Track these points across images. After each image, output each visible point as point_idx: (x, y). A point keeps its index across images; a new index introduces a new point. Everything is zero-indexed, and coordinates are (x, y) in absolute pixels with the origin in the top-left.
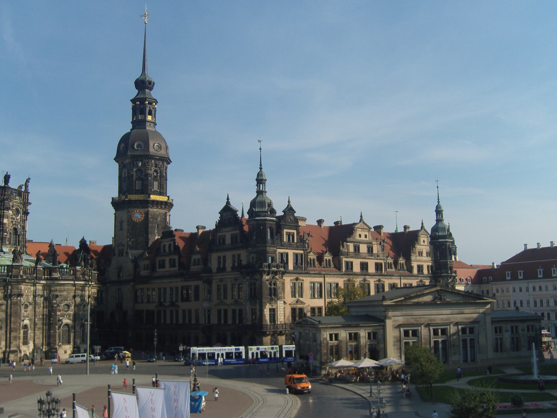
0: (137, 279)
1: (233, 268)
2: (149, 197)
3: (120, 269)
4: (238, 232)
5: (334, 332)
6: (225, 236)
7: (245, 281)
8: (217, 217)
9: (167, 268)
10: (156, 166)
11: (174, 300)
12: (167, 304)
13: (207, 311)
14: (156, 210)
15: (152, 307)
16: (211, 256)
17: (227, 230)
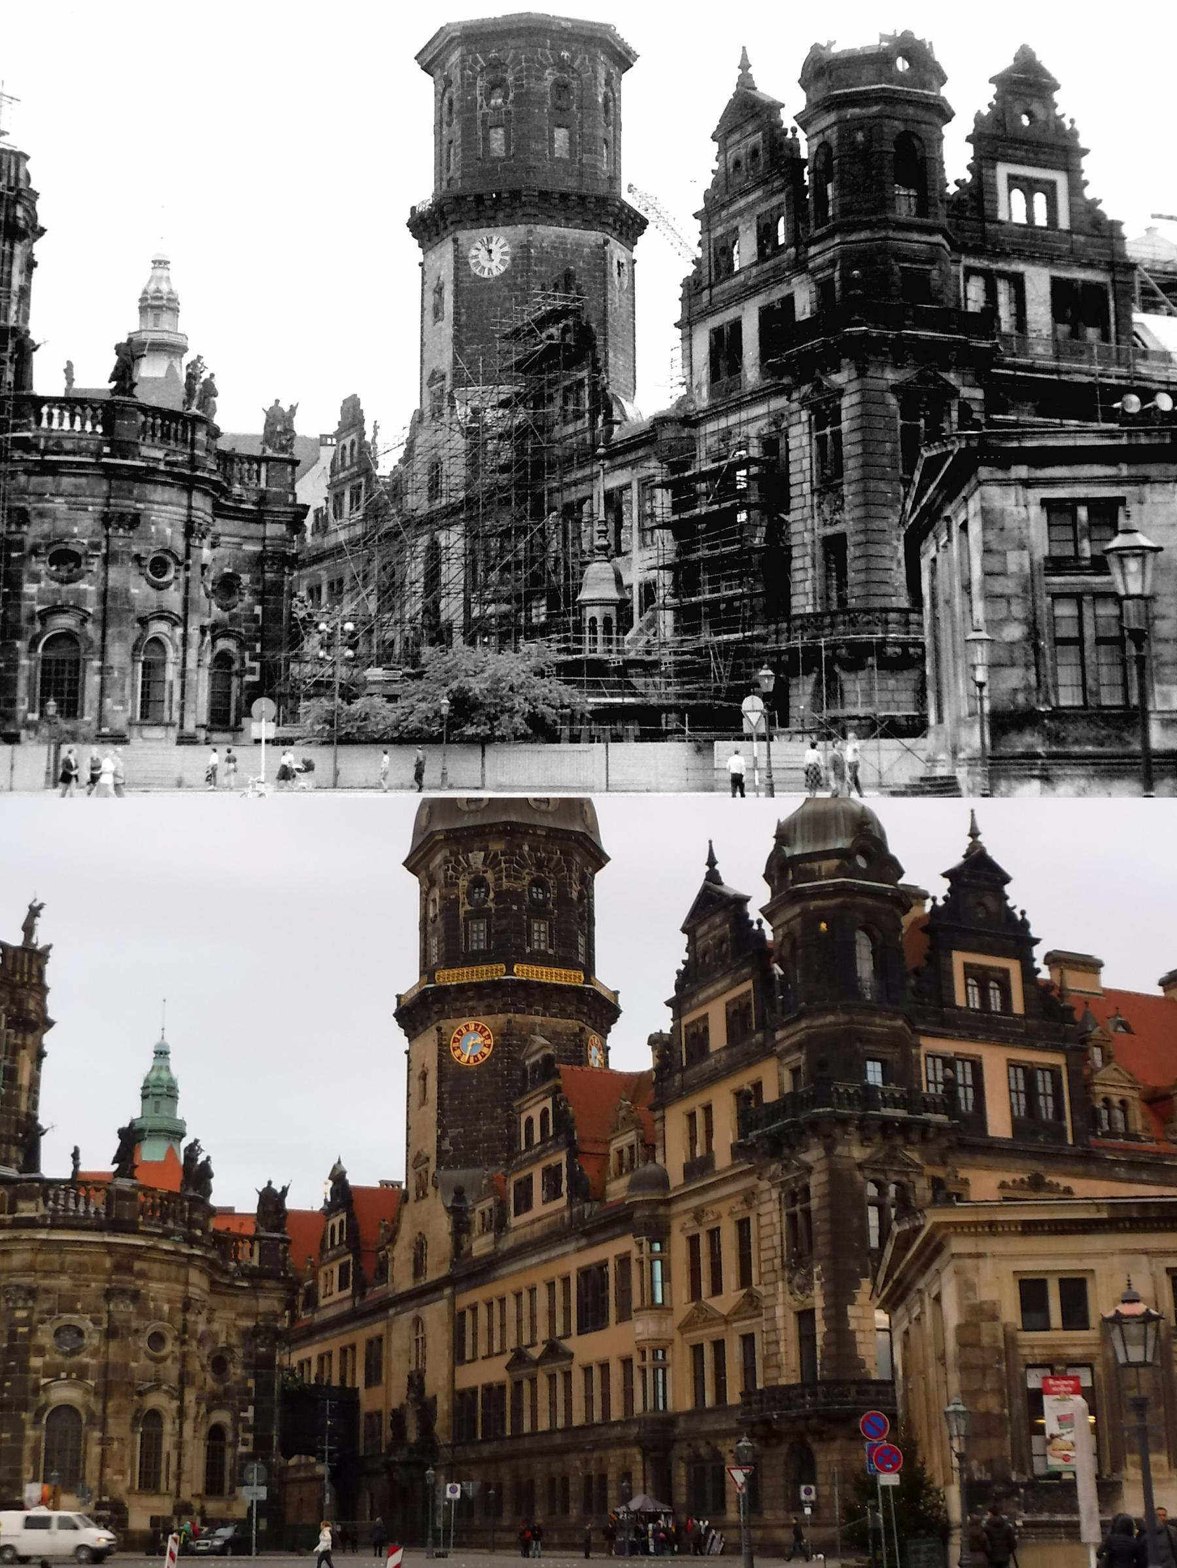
0: (469, 1272)
1: (738, 1151)
2: (510, 971)
3: (420, 1246)
4: (748, 985)
5: (1052, 1257)
6: (705, 1017)
7: (765, 1185)
8: (674, 953)
9: (540, 1208)
10: (540, 865)
11: (559, 1331)
12: (536, 1353)
13: (649, 1355)
14: (538, 1019)
15: (494, 1371)
16: (663, 1118)
17: (711, 991)
